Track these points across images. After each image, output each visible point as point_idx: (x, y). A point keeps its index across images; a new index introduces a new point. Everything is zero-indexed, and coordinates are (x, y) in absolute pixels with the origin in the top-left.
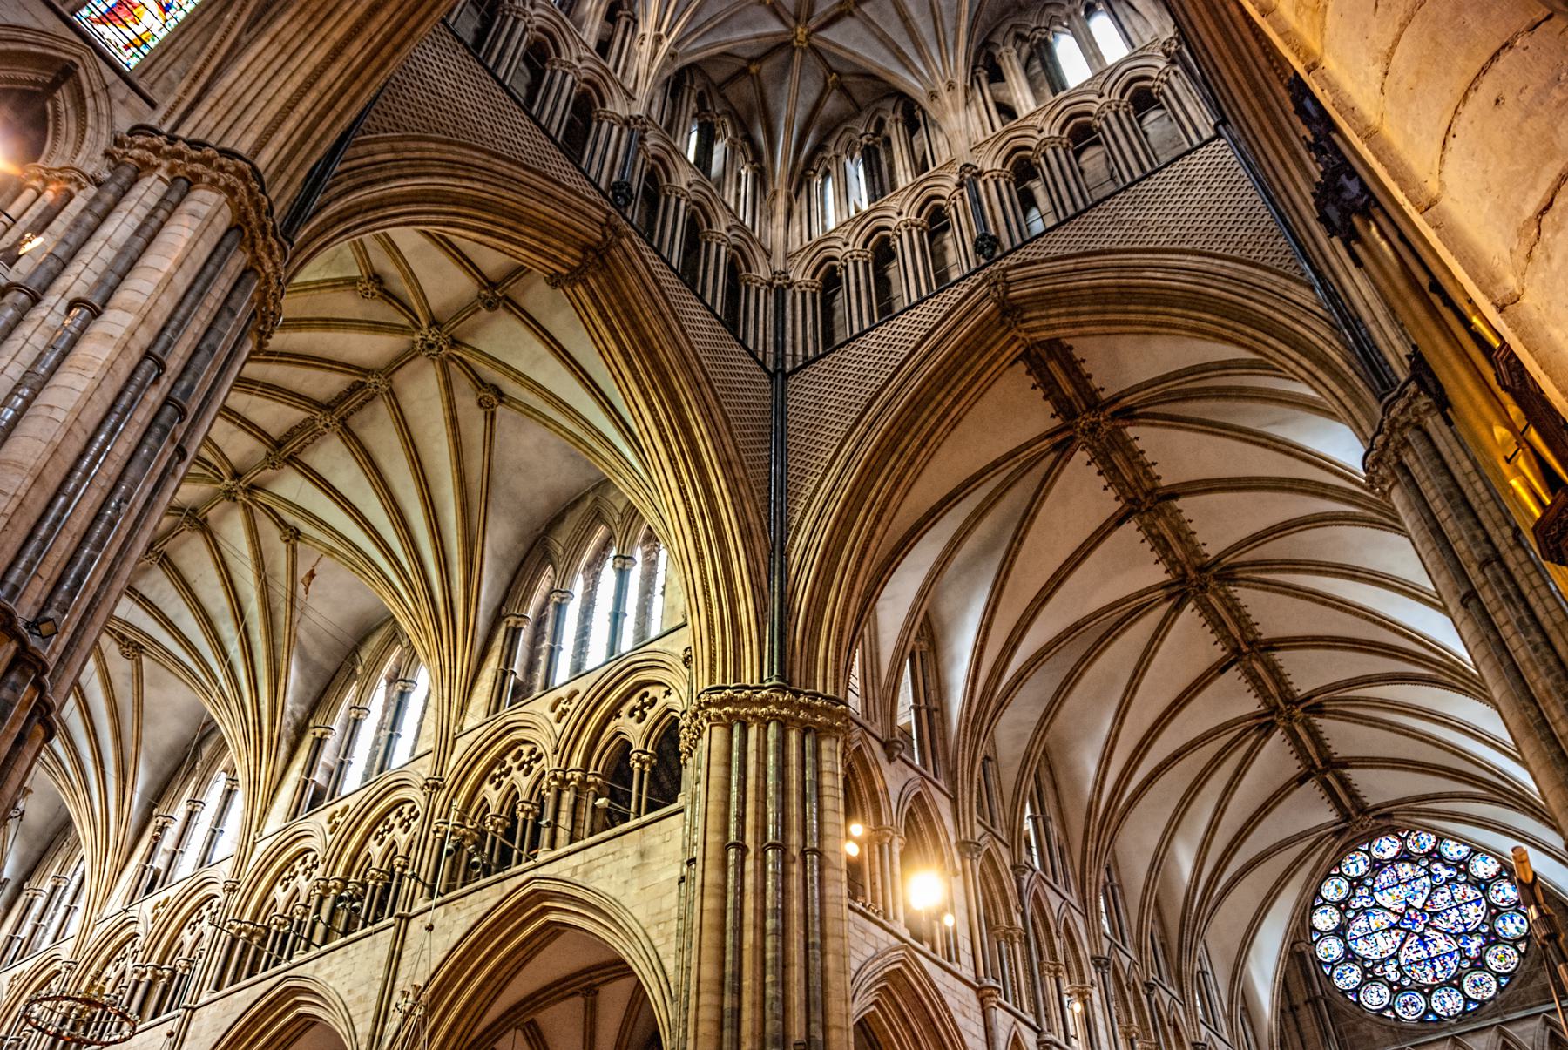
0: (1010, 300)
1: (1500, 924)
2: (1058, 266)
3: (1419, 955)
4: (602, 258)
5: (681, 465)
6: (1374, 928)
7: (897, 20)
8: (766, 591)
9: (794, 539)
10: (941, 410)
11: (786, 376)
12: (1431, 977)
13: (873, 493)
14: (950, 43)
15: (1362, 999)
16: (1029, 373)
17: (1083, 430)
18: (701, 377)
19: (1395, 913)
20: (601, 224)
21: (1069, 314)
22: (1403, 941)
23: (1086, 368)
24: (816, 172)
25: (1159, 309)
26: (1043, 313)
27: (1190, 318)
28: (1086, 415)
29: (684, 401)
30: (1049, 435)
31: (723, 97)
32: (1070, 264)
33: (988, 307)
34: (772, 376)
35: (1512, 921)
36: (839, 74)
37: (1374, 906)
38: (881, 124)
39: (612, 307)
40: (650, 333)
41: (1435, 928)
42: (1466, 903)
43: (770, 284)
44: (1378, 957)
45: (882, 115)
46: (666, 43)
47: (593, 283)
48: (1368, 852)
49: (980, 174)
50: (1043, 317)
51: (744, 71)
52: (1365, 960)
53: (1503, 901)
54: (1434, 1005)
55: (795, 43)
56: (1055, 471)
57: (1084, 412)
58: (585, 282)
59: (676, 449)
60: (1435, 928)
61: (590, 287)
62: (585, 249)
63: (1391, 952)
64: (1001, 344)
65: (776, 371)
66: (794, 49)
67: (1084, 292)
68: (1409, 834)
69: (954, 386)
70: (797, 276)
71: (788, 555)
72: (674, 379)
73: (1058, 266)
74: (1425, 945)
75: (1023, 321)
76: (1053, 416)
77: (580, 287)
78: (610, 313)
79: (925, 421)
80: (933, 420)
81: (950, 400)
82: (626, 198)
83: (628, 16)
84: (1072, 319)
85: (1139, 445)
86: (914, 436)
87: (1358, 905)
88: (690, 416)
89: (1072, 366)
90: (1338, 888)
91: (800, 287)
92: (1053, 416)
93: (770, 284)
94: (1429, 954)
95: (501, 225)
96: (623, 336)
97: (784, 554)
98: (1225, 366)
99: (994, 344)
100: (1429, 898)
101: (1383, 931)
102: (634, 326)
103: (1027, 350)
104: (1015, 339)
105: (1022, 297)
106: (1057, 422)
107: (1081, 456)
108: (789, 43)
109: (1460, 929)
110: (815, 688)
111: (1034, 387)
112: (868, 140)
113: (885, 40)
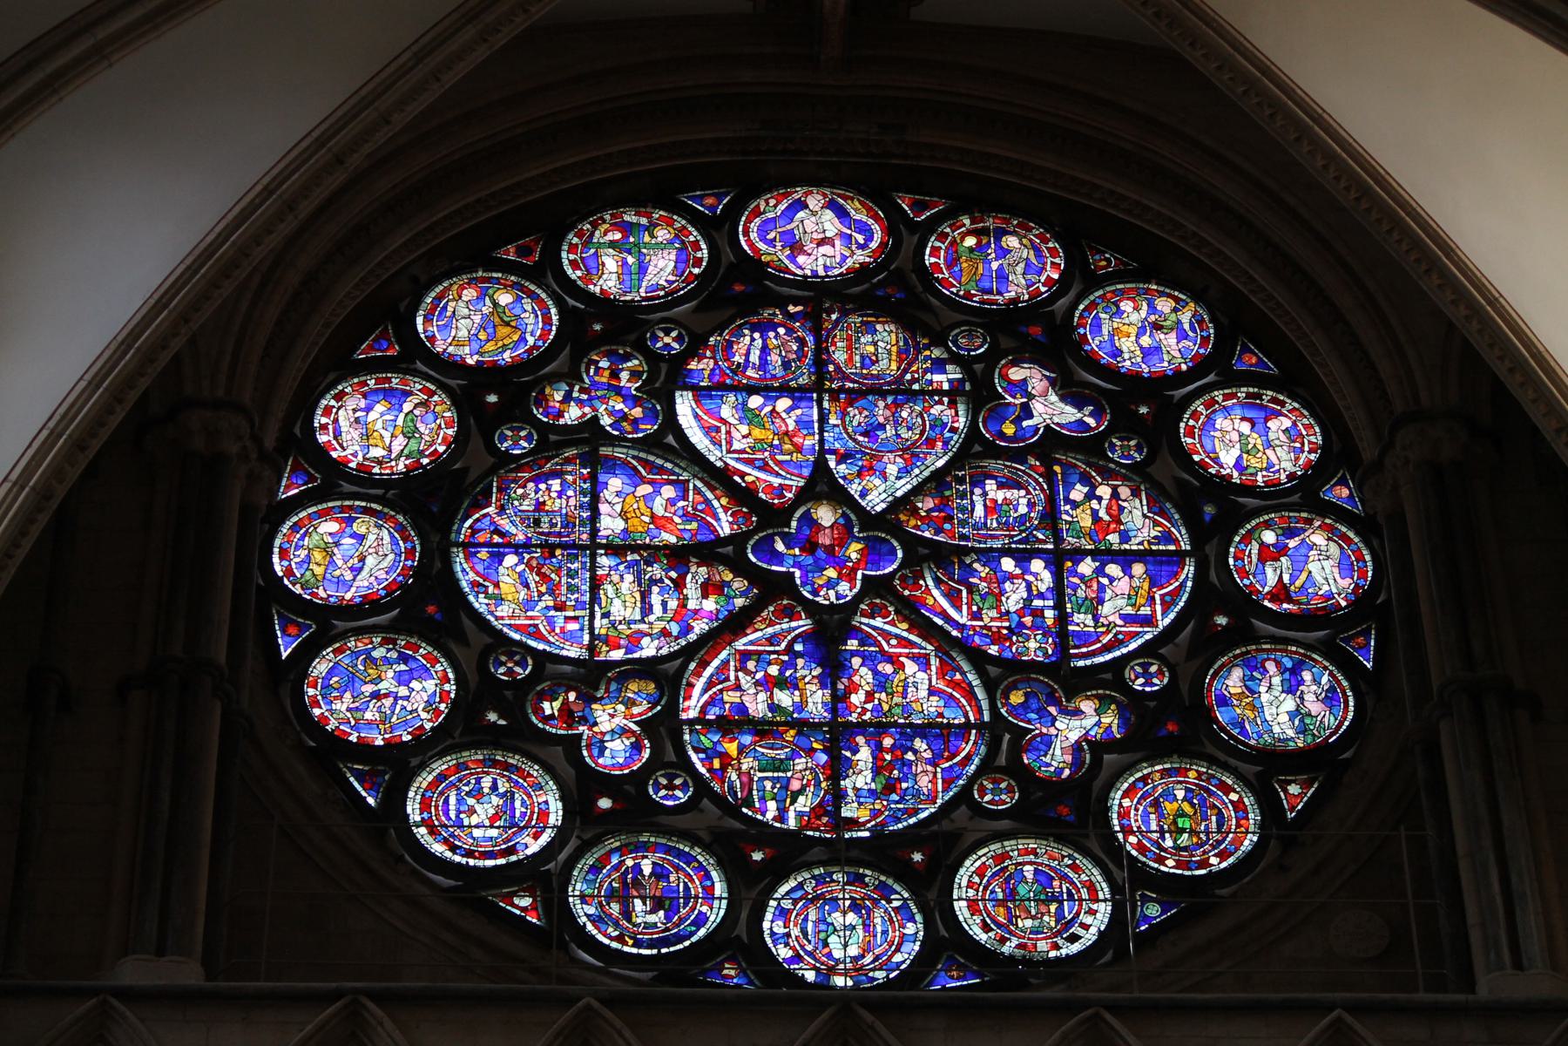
1: (1234, 681)
3: (784, 698)
6: (610, 525)
12: (804, 803)
15: (413, 810)
19: (742, 496)
22: (734, 624)
35: (1293, 686)
37: (651, 443)
41: (912, 612)
42: (1105, 555)
44: (573, 652)
48: (720, 229)
52: (499, 642)
53: (1281, 592)
54: (770, 924)
60: (912, 612)
63: (648, 649)
68: (950, 215)
74: (833, 670)
87: (573, 414)
90: (500, 319)
94: (838, 701)
100: (937, 482)
101: (654, 553)
109: (1034, 647)
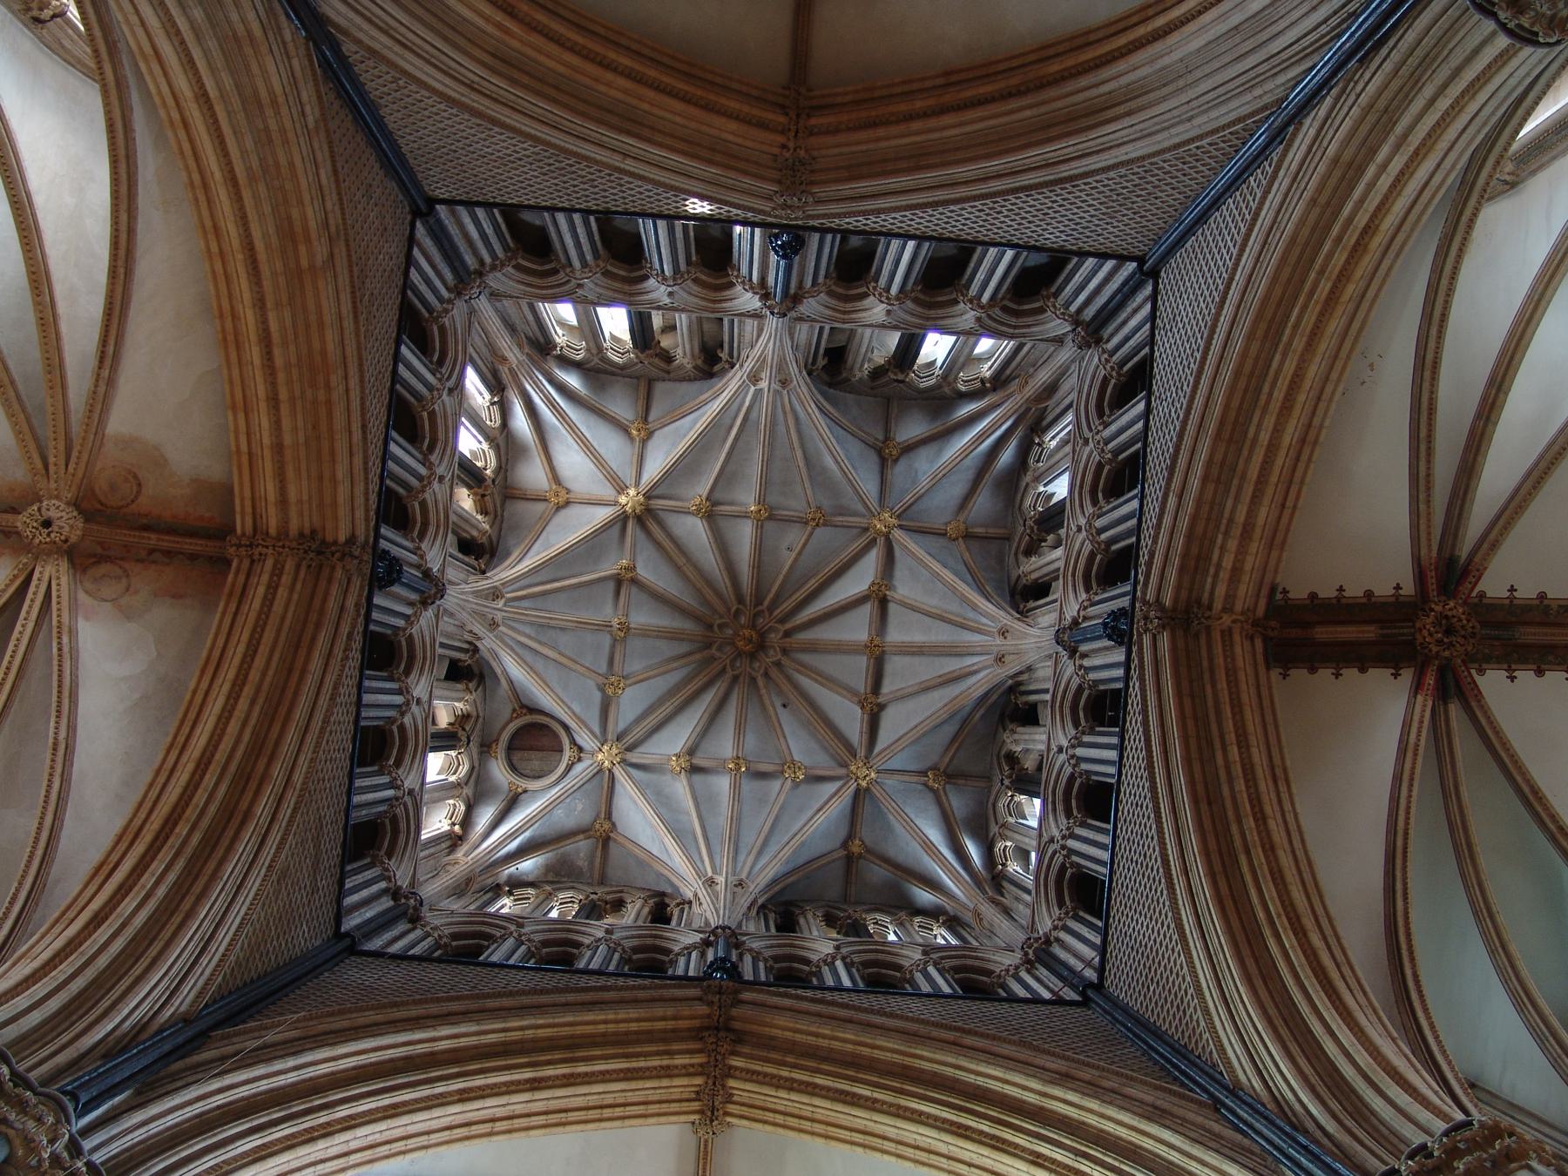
0: (1174, 609)
2: (1167, 520)
4: (729, 1030)
5: (1007, 1135)
7: (916, 660)
8: (1246, 1142)
9: (1228, 1063)
10: (1237, 770)
11: (1099, 987)
13: (1261, 915)
14: (971, 615)
16: (1313, 670)
17: (1439, 642)
18: (950, 1035)
20: (700, 999)
21: (1226, 534)
23: (1354, 591)
24: (1003, 865)
25: (1266, 389)
26: (1212, 571)
27: (1290, 343)
28: (1418, 625)
29: (950, 1071)
30: (1417, 687)
31: (857, 903)
32: (1172, 501)
33: (1165, 640)
34: (1085, 1002)
36: (931, 769)
38: (1012, 759)
39: (784, 1064)
40: (849, 1047)
43: (1028, 962)
45: (1003, 753)
46: (721, 879)
47: (737, 1062)
49: (1075, 622)
50: (1216, 575)
51: (850, 860)
55: (864, 784)
56: (1483, 721)
57: (1414, 627)
58: (730, 1072)
59: (985, 1127)
61: (742, 1070)
62: (696, 1034)
64: (1218, 649)
65: (1083, 994)
66: (867, 790)
67: (1209, 495)
69: (1222, 737)
70: (1045, 925)
71: (1237, 1082)
72: (918, 1063)
73: (1167, 520)
75: (1210, 608)
76: (1396, 676)
77: (732, 1083)
78: (785, 1073)
79: (1234, 798)
80: (1240, 785)
81: (1234, 752)
82: (725, 970)
83: (678, 905)
84: (1237, 531)
85: (1526, 592)
86: (1239, 821)
88: (971, 1078)
89: (1341, 609)
91: (1055, 928)
92: (1396, 676)
93: (1028, 962)
95: (549, 1063)
96: (820, 1080)
97: (1235, 1090)
98: (1427, 365)
99: (1211, 660)
102: (825, 1059)
103: (1266, 639)
104: (1227, 634)
105: (1178, 588)
106: (1407, 675)
107: (1492, 683)
108: (858, 791)
110: (1406, 1142)
111: (1337, 675)
112: (1010, 777)
113: (927, 688)
